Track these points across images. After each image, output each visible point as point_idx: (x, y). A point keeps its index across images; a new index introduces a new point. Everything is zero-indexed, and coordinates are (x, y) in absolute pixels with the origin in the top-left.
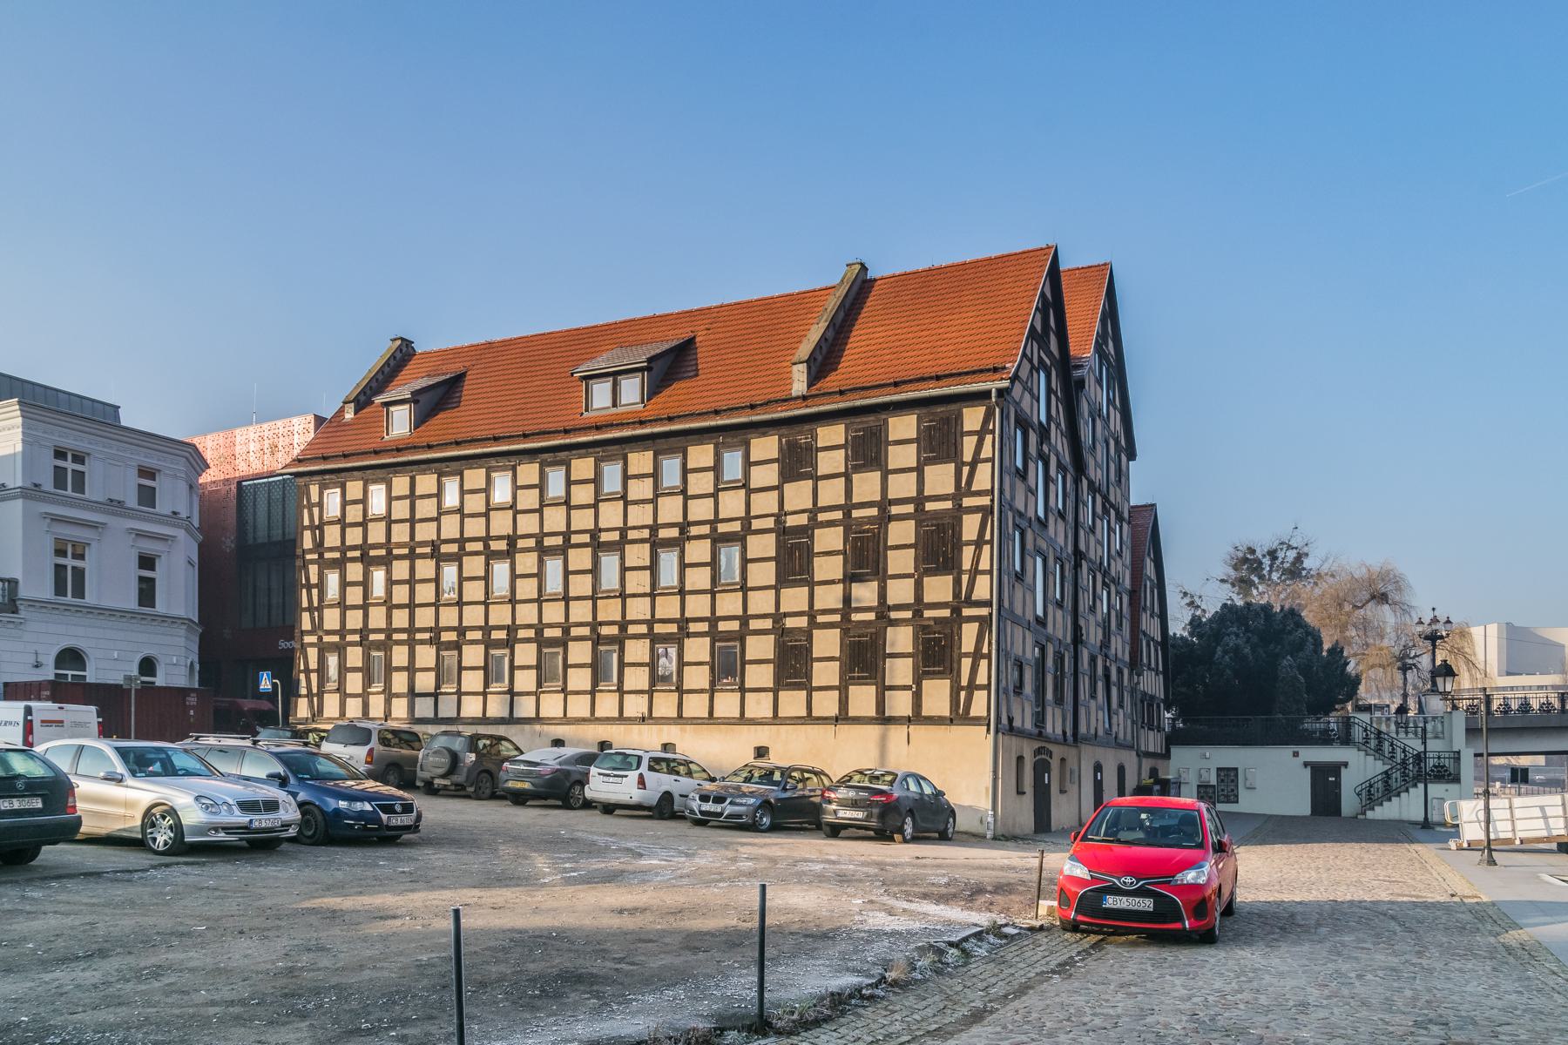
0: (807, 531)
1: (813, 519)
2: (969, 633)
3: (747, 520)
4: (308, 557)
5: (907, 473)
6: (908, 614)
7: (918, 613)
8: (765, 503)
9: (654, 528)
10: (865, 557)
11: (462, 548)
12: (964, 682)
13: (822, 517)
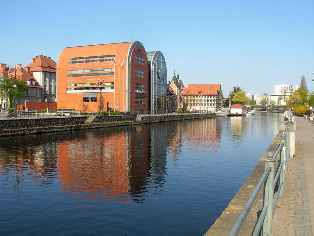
5: (212, 98)
10: (211, 101)
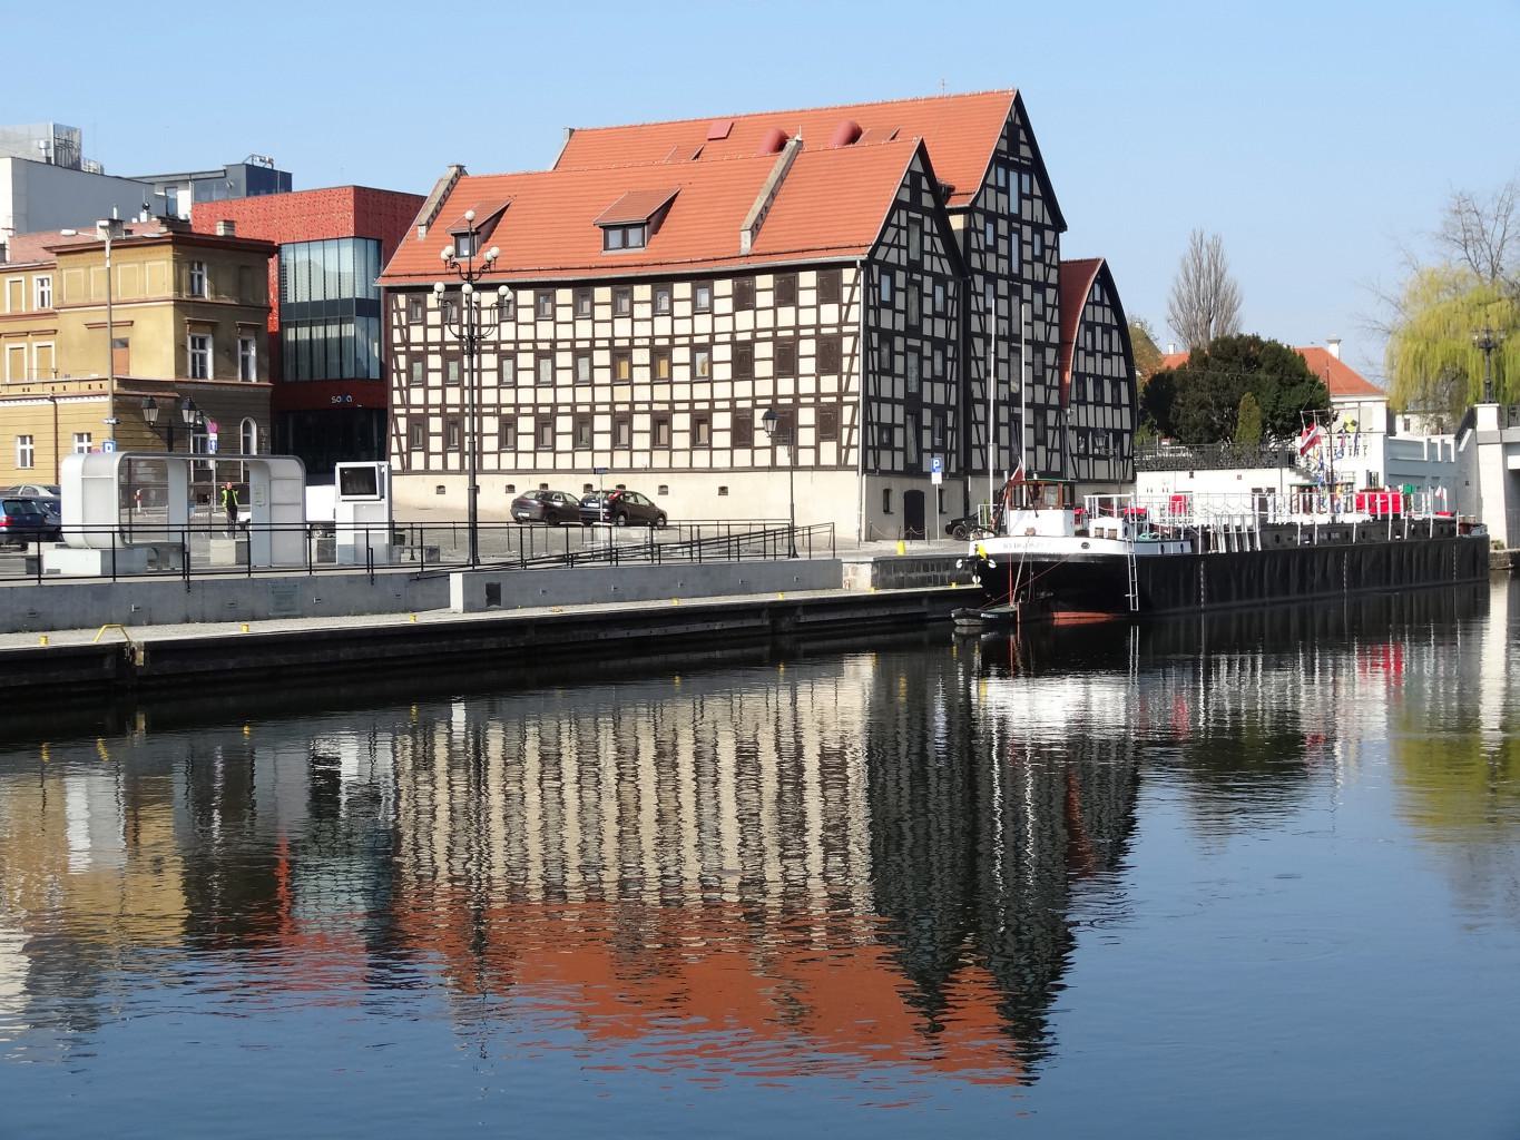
0: (749, 345)
1: (754, 336)
2: (847, 412)
3: (712, 335)
4: (396, 349)
6: (812, 400)
7: (818, 399)
8: (724, 325)
9: (652, 338)
10: (786, 362)
11: (517, 347)
12: (844, 443)
13: (759, 335)
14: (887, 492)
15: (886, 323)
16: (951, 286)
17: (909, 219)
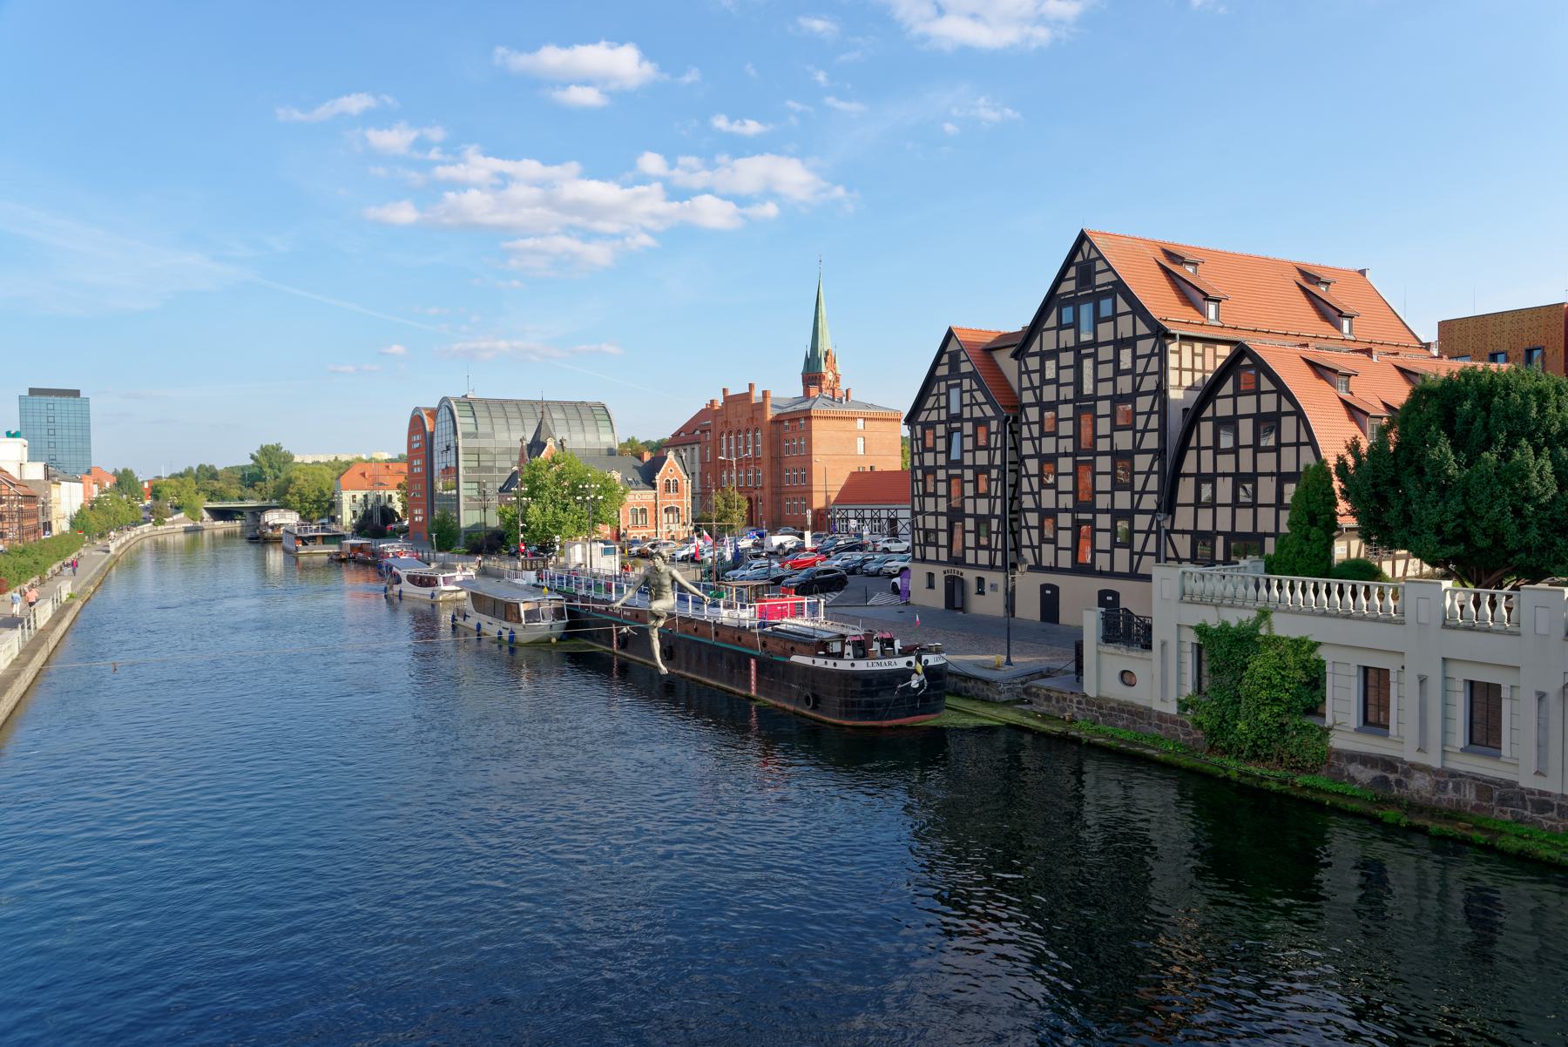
14: (931, 576)
15: (929, 459)
16: (994, 425)
17: (949, 387)
